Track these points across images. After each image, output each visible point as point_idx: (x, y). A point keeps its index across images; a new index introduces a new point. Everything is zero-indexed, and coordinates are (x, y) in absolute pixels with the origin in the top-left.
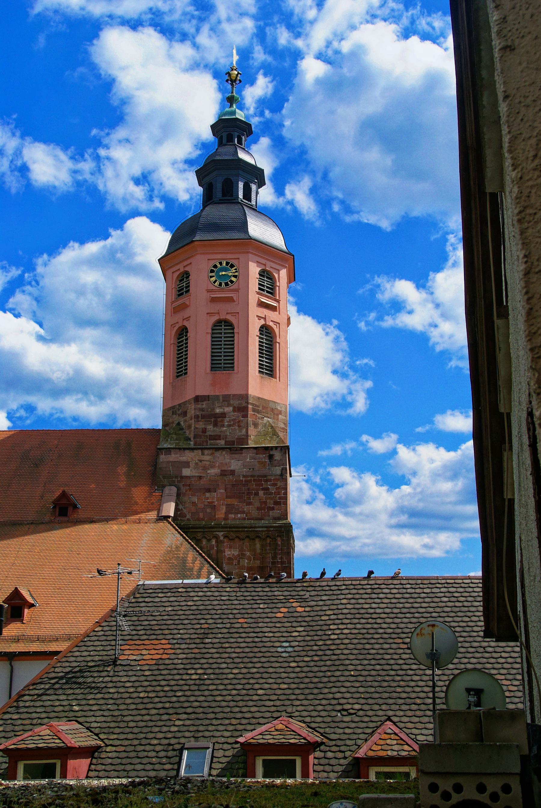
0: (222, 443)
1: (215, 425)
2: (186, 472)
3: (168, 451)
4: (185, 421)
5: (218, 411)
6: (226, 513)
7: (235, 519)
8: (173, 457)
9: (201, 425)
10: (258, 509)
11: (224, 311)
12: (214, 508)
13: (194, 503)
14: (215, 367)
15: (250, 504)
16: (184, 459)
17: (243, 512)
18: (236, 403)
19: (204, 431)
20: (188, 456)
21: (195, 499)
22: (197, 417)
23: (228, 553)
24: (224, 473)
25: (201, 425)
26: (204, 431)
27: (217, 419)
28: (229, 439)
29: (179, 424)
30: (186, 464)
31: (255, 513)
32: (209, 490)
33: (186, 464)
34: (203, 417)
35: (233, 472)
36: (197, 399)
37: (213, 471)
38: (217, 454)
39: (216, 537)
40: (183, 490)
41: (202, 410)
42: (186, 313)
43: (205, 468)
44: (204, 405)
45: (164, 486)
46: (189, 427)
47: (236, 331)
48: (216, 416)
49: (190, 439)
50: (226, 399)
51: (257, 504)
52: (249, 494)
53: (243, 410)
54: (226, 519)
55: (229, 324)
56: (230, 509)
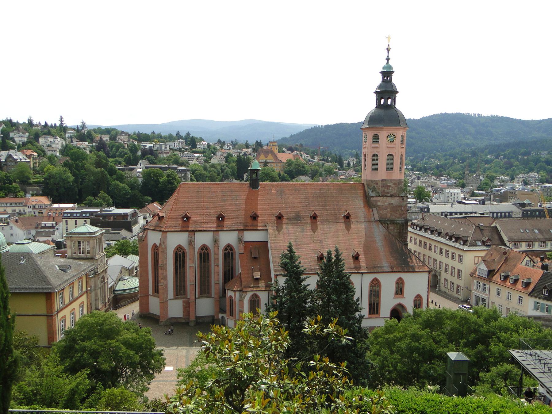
2: (379, 204)
3: (373, 197)
7: (392, 218)
8: (375, 199)
18: (394, 182)
20: (379, 198)
23: (390, 228)
24: (389, 204)
25: (383, 189)
30: (379, 201)
31: (398, 216)
33: (379, 201)
36: (382, 180)
37: (386, 204)
42: (378, 150)
43: (384, 202)
46: (379, 189)
50: (391, 181)
55: (392, 155)
56: (391, 216)
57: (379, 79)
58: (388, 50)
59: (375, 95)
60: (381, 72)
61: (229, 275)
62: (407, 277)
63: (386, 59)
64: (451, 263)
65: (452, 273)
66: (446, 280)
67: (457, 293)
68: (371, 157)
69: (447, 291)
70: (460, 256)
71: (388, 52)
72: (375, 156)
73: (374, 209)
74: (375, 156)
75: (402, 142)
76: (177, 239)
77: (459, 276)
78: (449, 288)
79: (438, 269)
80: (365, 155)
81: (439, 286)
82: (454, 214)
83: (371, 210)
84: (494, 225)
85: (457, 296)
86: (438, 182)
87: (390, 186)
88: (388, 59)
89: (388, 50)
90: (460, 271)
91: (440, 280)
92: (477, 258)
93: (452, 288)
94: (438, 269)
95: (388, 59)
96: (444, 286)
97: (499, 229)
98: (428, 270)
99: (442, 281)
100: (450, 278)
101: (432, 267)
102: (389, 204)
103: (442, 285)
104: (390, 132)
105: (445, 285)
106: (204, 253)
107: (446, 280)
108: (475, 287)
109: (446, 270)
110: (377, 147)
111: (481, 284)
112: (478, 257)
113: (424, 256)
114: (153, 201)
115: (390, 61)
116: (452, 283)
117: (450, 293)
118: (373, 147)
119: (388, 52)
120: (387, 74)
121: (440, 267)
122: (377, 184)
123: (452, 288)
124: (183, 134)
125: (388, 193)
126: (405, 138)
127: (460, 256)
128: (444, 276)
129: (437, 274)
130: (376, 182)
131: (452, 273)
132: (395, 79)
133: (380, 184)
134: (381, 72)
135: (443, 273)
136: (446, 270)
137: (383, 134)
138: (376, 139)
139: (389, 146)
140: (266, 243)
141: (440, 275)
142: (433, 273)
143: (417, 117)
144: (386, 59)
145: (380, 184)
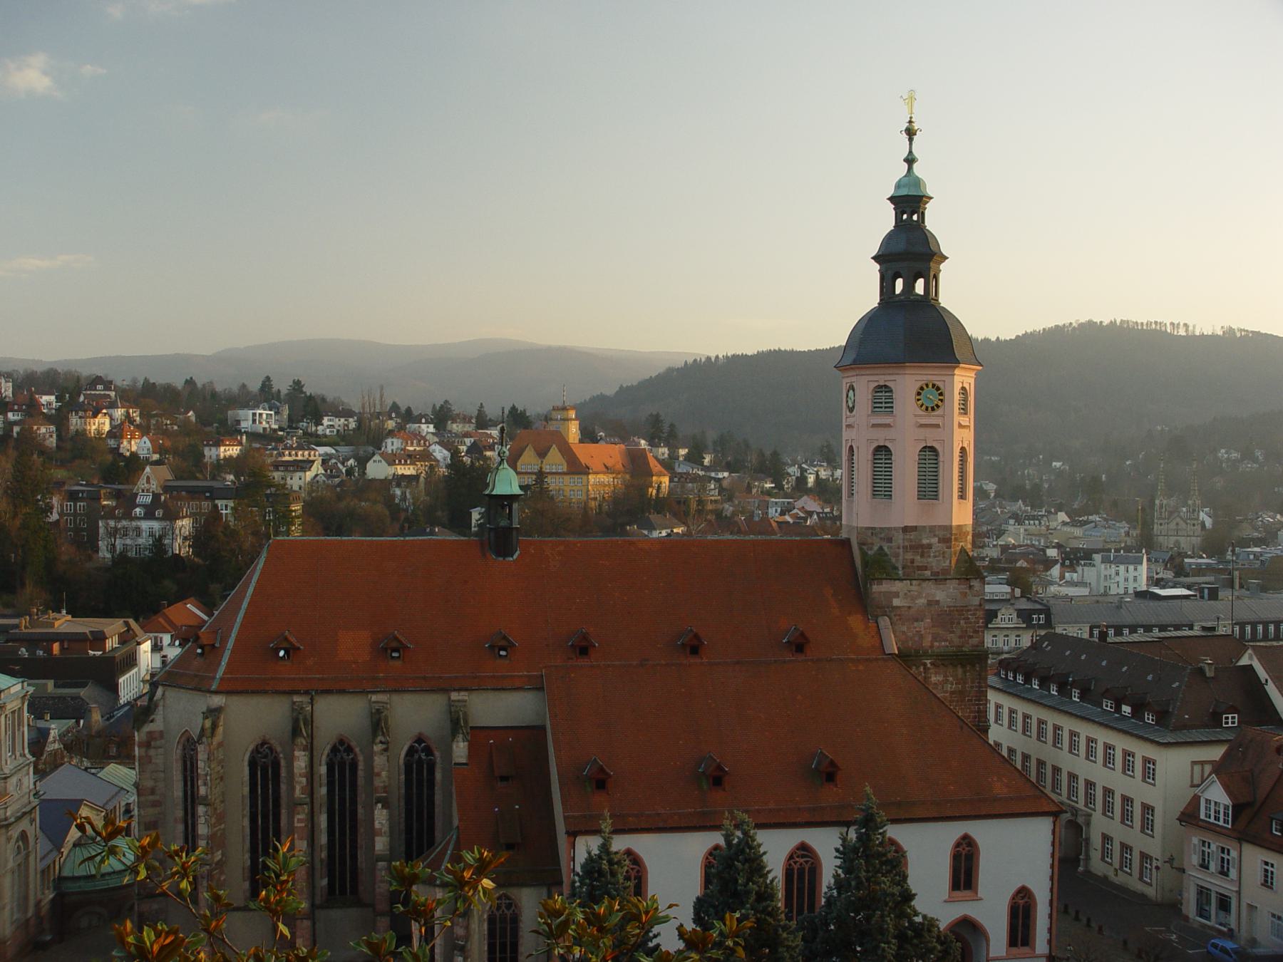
0: (928, 573)
1: (922, 556)
2: (896, 602)
4: (890, 548)
5: (925, 541)
6: (932, 642)
7: (940, 646)
9: (909, 556)
10: (960, 637)
11: (931, 438)
12: (921, 637)
13: (904, 633)
14: (922, 495)
15: (952, 632)
16: (894, 589)
17: (946, 640)
18: (941, 534)
19: (912, 561)
21: (905, 629)
22: (905, 548)
23: (934, 679)
24: (930, 603)
25: (909, 556)
26: (912, 561)
27: (923, 549)
28: (936, 570)
29: (881, 548)
30: (897, 595)
31: (956, 641)
32: (917, 620)
33: (897, 595)
34: (912, 547)
35: (938, 602)
36: (906, 529)
37: (922, 601)
38: (925, 584)
39: (925, 665)
40: (895, 619)
41: (911, 540)
43: (913, 599)
44: (913, 535)
45: (877, 617)
46: (897, 555)
47: (941, 458)
48: (922, 546)
49: (896, 568)
50: (932, 530)
51: (959, 632)
52: (952, 623)
53: (946, 541)
54: (932, 647)
55: (932, 449)
57: (886, 220)
58: (910, 133)
59: (878, 267)
60: (892, 199)
61: (417, 835)
62: (986, 833)
63: (906, 160)
64: (1121, 784)
65: (1126, 816)
66: (1106, 838)
67: (1141, 879)
68: (870, 457)
69: (1111, 874)
70: (1146, 760)
71: (911, 140)
72: (882, 452)
73: (884, 622)
74: (882, 452)
75: (964, 411)
76: (253, 718)
77: (1147, 825)
78: (1117, 866)
79: (1081, 805)
80: (851, 447)
81: (1088, 858)
82: (1126, 631)
83: (872, 623)
84: (1244, 661)
85: (1139, 887)
86: (1078, 532)
87: (930, 546)
88: (910, 160)
89: (910, 133)
90: (1148, 809)
91: (1087, 840)
92: (1197, 768)
93: (1125, 862)
94: (1081, 805)
95: (910, 160)
96: (1103, 859)
97: (1262, 674)
98: (1054, 809)
99: (1096, 841)
100: (1118, 832)
101: (1064, 798)
102: (930, 603)
103: (1096, 855)
104: (925, 378)
105: (1105, 853)
106: (342, 764)
107: (1106, 838)
108: (1195, 860)
109: (1107, 808)
110: (888, 426)
111: (1213, 847)
112: (1202, 763)
113: (1041, 763)
114: (181, 597)
115: (915, 166)
116: (1125, 848)
117: (1121, 879)
118: (874, 426)
119: (911, 140)
120: (909, 202)
121: (1090, 799)
122: (890, 540)
123: (1125, 862)
124: (282, 385)
125: (926, 568)
126: (971, 399)
127: (1146, 760)
128: (1099, 825)
129: (1080, 820)
130: (886, 534)
131: (1126, 816)
132: (935, 220)
133: (899, 539)
134: (892, 199)
135: (1097, 816)
136: (1107, 808)
137: (906, 383)
138: (883, 398)
139: (923, 421)
140: (543, 728)
141: (1088, 824)
142: (1066, 817)
143: (1008, 334)
144: (906, 160)
145: (899, 539)
